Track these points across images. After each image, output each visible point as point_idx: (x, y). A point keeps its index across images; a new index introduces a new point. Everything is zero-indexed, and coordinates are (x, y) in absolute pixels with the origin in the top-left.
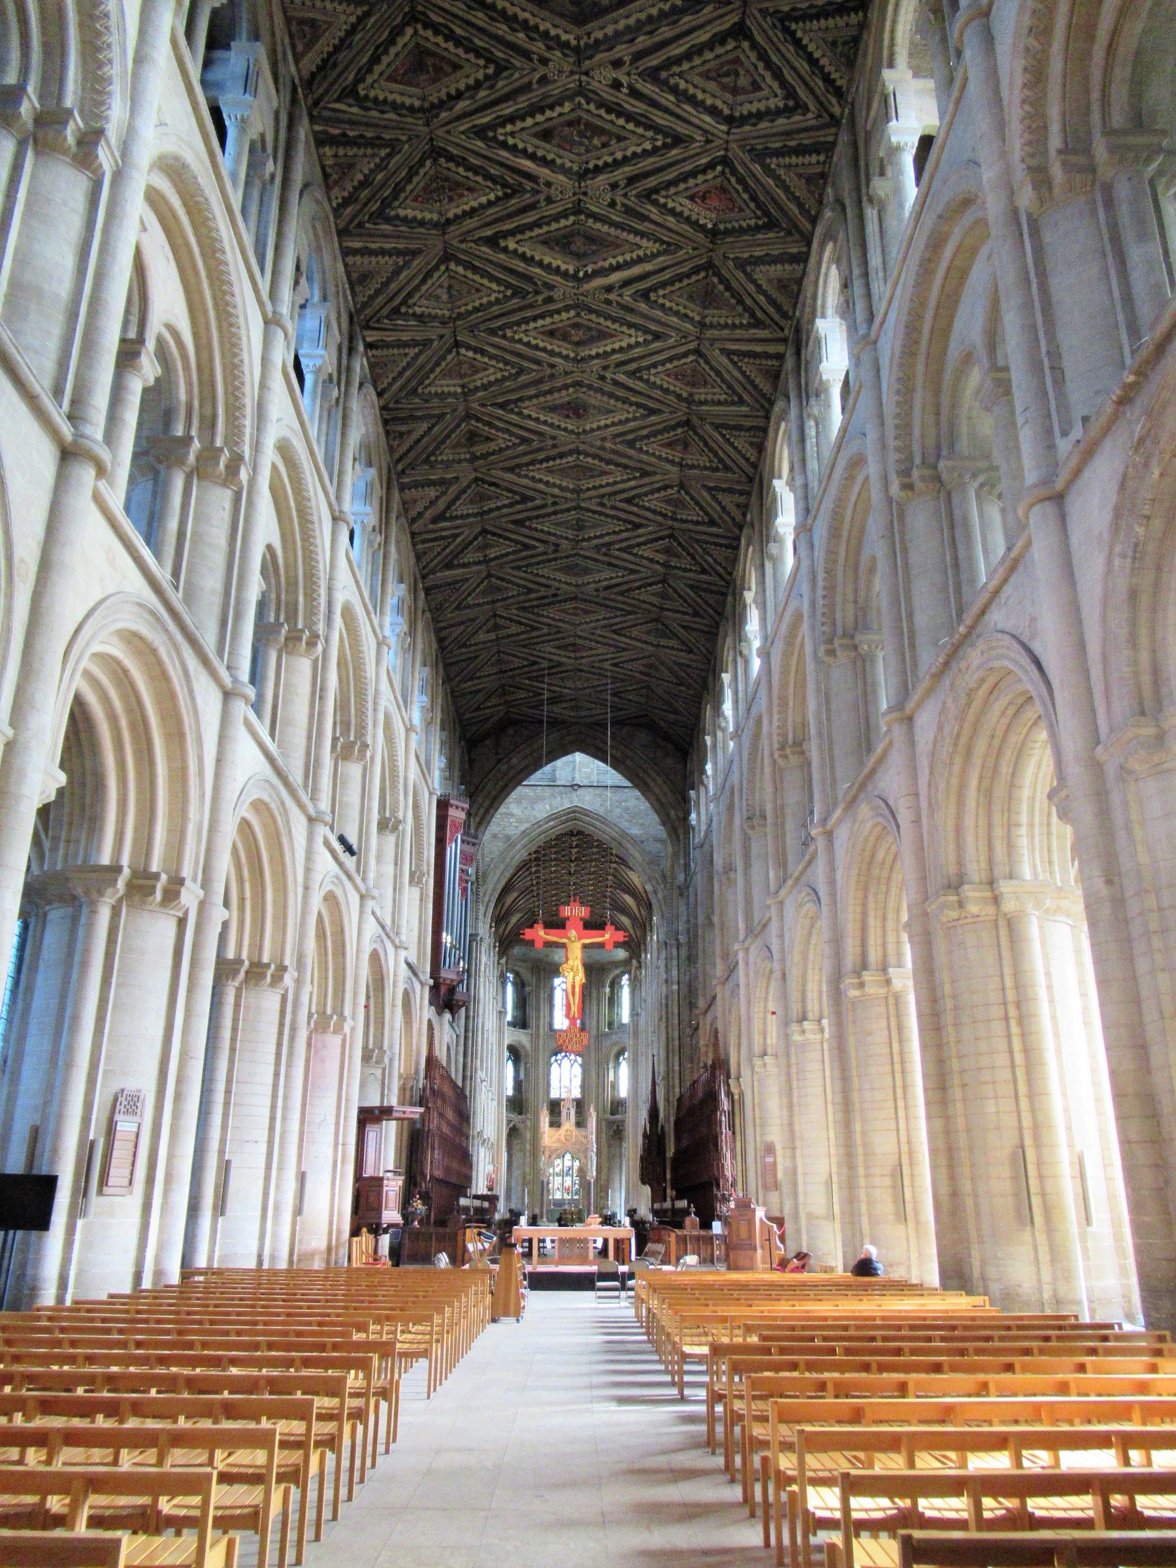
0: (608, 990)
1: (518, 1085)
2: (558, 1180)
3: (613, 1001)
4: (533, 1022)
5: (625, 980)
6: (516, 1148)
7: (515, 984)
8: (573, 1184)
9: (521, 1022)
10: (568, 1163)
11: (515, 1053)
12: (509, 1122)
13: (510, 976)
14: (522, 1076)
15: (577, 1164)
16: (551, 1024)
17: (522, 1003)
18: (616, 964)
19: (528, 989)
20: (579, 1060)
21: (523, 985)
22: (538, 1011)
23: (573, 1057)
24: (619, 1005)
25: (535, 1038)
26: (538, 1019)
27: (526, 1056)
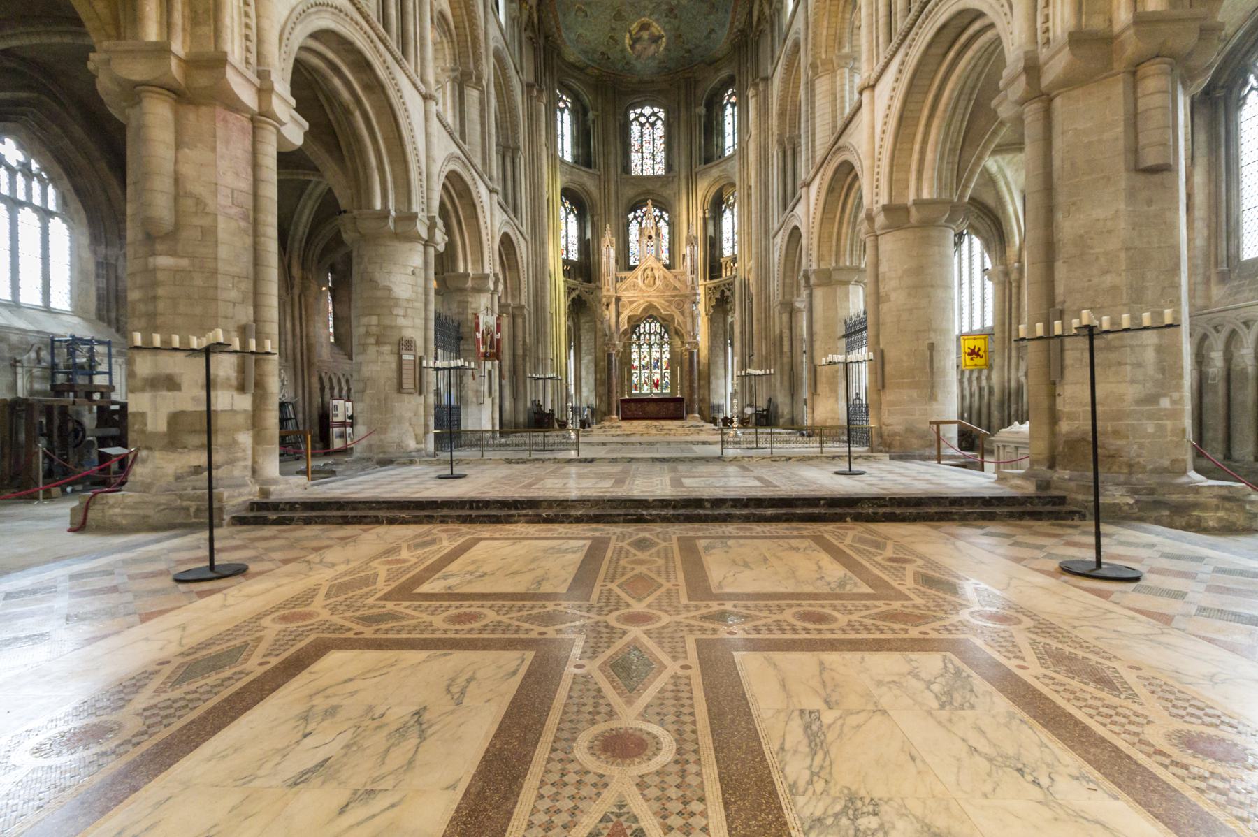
0: (702, 110)
1: (584, 246)
2: (645, 373)
3: (712, 128)
4: (600, 161)
5: (730, 97)
6: (585, 327)
7: (573, 112)
8: (663, 377)
9: (584, 158)
10: (656, 355)
11: (576, 200)
12: (570, 290)
13: (566, 101)
14: (589, 235)
15: (667, 355)
16: (626, 168)
17: (582, 137)
18: (713, 63)
19: (591, 115)
20: (666, 216)
21: (585, 113)
22: (605, 143)
23: (657, 213)
24: (722, 133)
25: (603, 182)
26: (606, 155)
27: (593, 206)
